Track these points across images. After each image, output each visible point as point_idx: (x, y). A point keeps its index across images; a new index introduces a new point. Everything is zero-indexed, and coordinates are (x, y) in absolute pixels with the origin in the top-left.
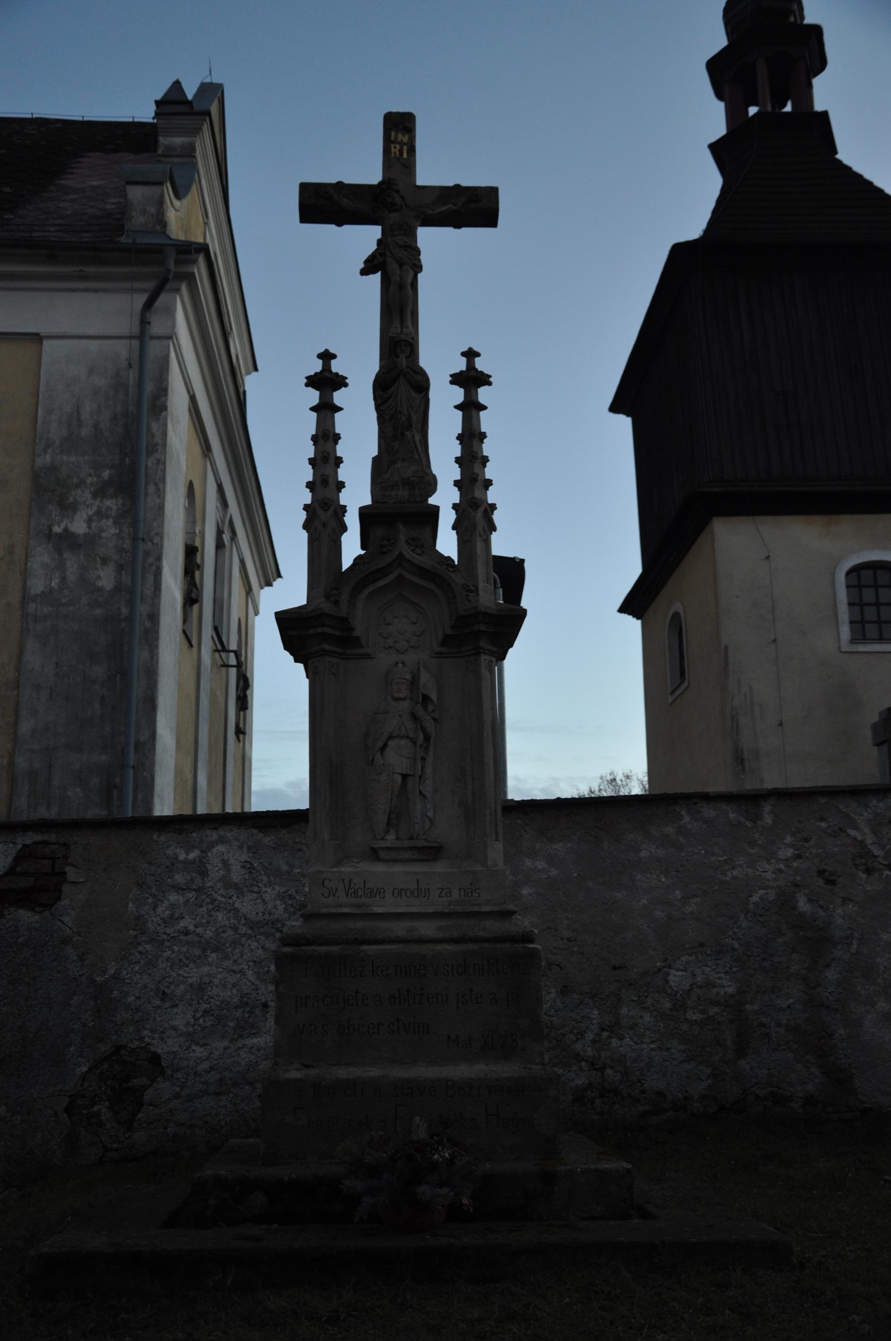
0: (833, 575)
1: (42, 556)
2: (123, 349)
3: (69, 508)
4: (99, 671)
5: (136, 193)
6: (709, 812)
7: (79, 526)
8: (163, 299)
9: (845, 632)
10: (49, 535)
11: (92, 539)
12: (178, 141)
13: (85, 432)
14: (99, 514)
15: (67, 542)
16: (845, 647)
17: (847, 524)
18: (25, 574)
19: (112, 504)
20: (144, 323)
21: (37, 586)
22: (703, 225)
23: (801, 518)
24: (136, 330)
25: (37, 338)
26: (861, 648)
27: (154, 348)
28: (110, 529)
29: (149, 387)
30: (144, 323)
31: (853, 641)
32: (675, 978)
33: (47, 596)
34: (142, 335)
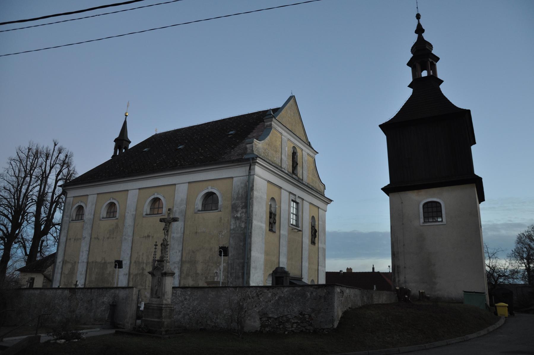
0: (419, 206)
1: (233, 221)
2: (246, 178)
3: (237, 211)
4: (242, 244)
5: (248, 146)
6: (231, 289)
7: (239, 215)
8: (252, 167)
9: (422, 220)
10: (234, 217)
11: (241, 217)
12: (269, 123)
13: (240, 196)
14: (242, 212)
15: (237, 218)
16: (421, 224)
17: (423, 192)
18: (230, 225)
19: (244, 210)
20: (249, 173)
21: (232, 227)
22: (442, 90)
23: (411, 192)
24: (247, 174)
25: (232, 178)
26: (426, 224)
27: (252, 177)
28: (244, 215)
29: (251, 185)
30: (249, 173)
31: (425, 222)
32: (225, 312)
33: (233, 229)
34: (249, 175)
